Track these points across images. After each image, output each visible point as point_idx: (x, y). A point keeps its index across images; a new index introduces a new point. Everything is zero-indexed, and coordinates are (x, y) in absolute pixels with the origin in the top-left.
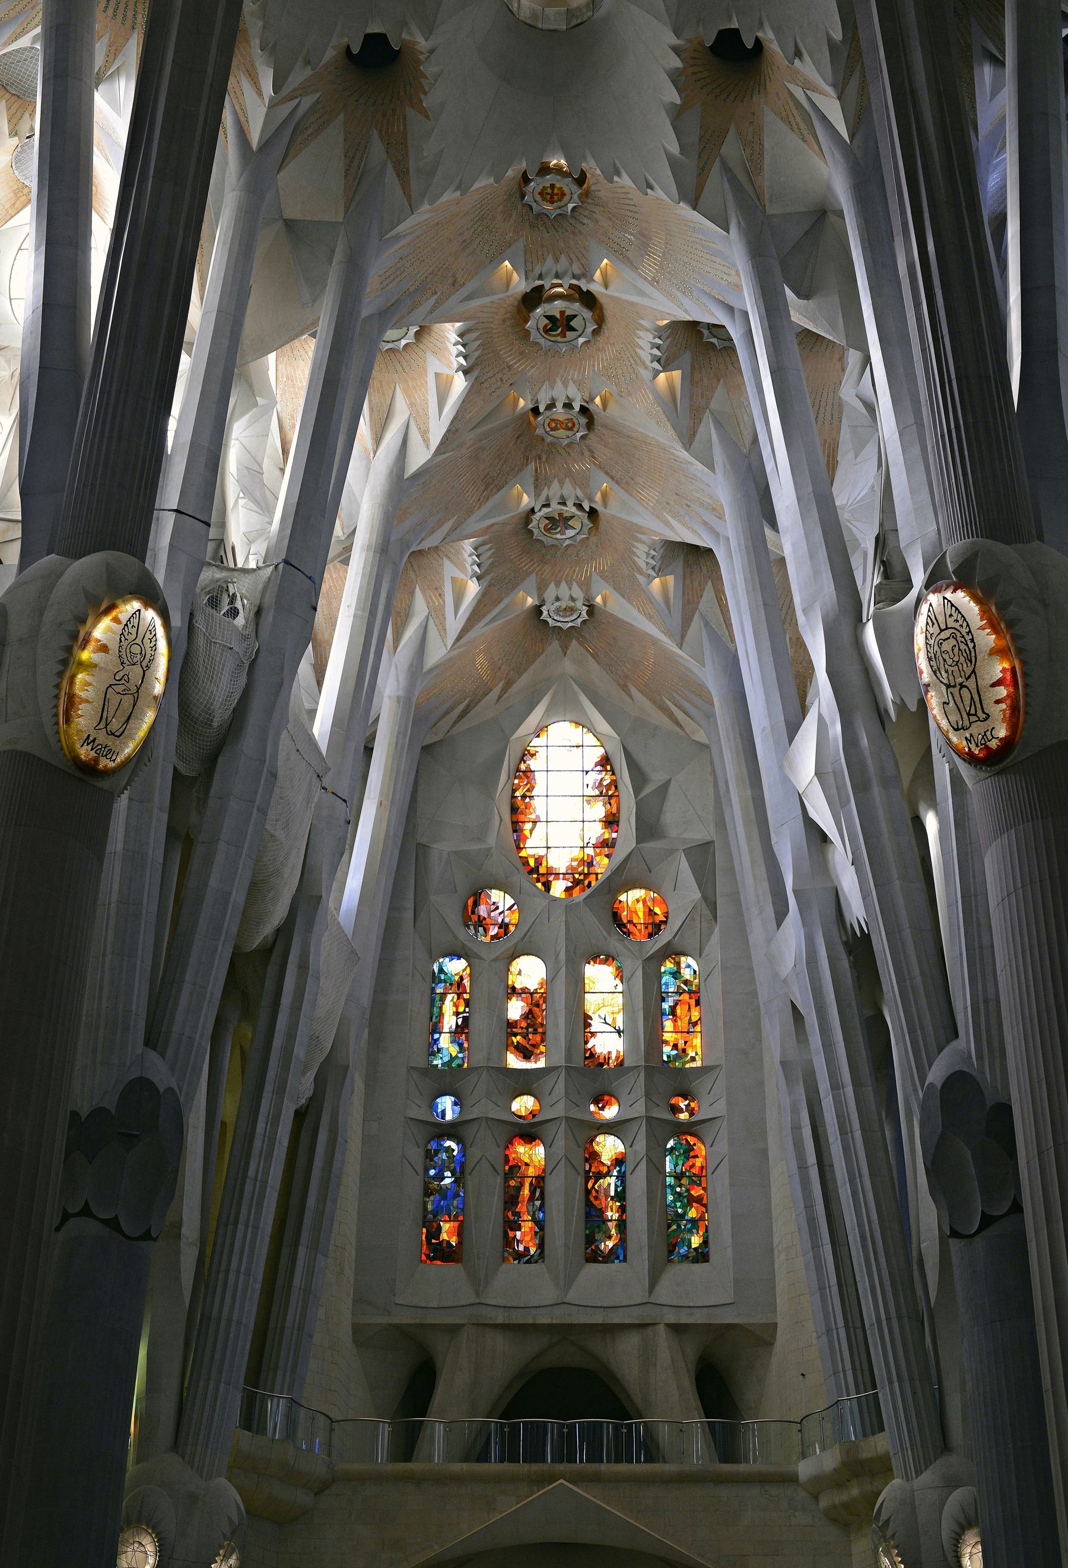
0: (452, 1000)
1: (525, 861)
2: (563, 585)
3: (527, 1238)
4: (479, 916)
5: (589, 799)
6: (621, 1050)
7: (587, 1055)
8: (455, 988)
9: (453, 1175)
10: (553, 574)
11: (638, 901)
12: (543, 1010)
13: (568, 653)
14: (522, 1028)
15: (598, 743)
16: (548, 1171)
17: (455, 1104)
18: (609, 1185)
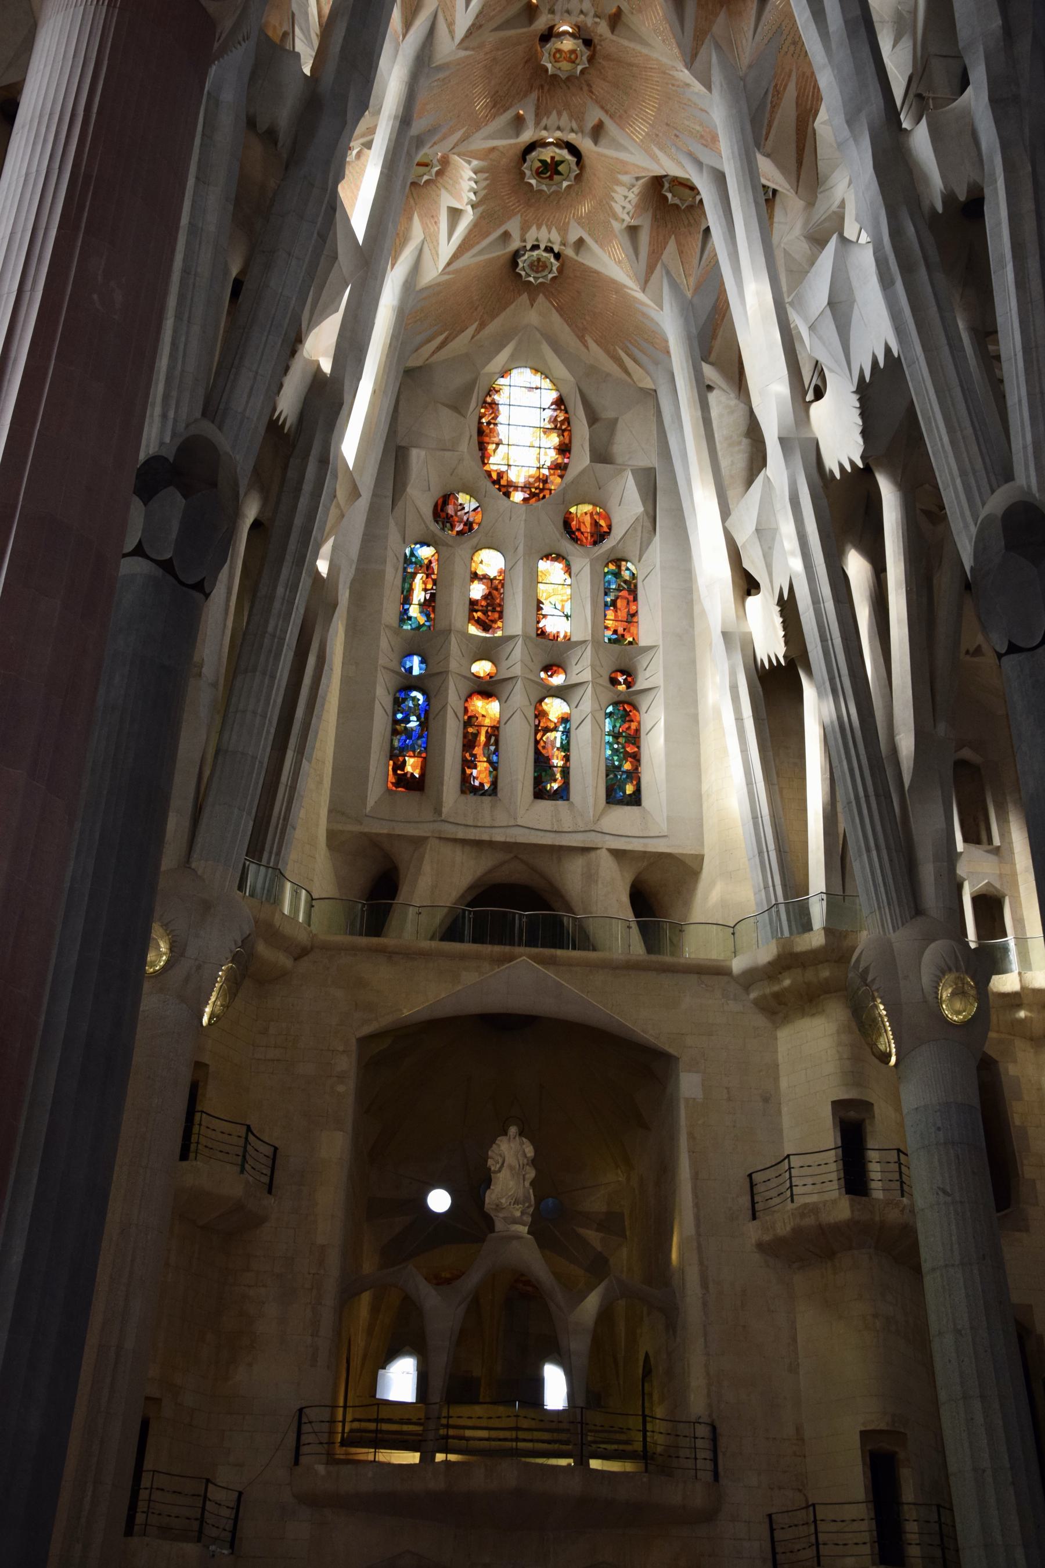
0: (422, 579)
1: (489, 474)
2: (544, 229)
3: (482, 776)
4: (447, 514)
5: (546, 431)
6: (569, 631)
7: (539, 632)
8: (425, 568)
9: (418, 719)
10: (535, 218)
11: (586, 513)
12: (501, 594)
13: (534, 305)
14: (482, 606)
15: (554, 388)
16: (502, 723)
17: (421, 662)
18: (555, 738)
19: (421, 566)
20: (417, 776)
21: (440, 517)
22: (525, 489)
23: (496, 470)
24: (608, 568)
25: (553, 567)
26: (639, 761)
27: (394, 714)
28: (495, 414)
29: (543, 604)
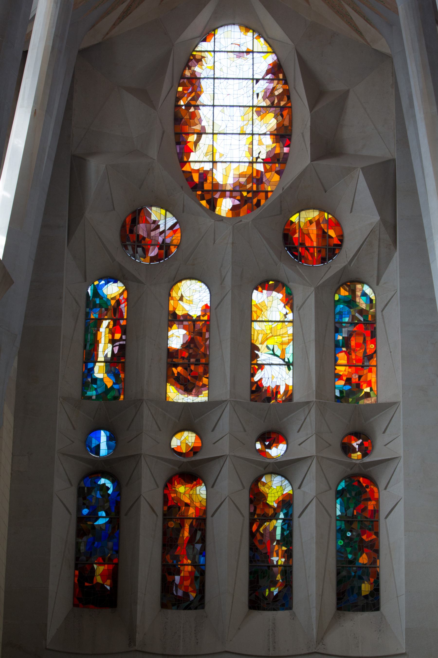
0: (108, 327)
1: (188, 175)
3: (187, 583)
4: (138, 235)
6: (290, 383)
7: (254, 388)
8: (110, 313)
9: (107, 515)
11: (311, 222)
15: (270, 50)
16: (209, 513)
17: (109, 439)
18: (275, 528)
19: (107, 309)
20: (108, 588)
21: (129, 241)
22: (234, 194)
23: (198, 170)
24: (339, 294)
25: (270, 298)
26: (377, 551)
27: (79, 510)
28: (196, 92)
29: (258, 350)
